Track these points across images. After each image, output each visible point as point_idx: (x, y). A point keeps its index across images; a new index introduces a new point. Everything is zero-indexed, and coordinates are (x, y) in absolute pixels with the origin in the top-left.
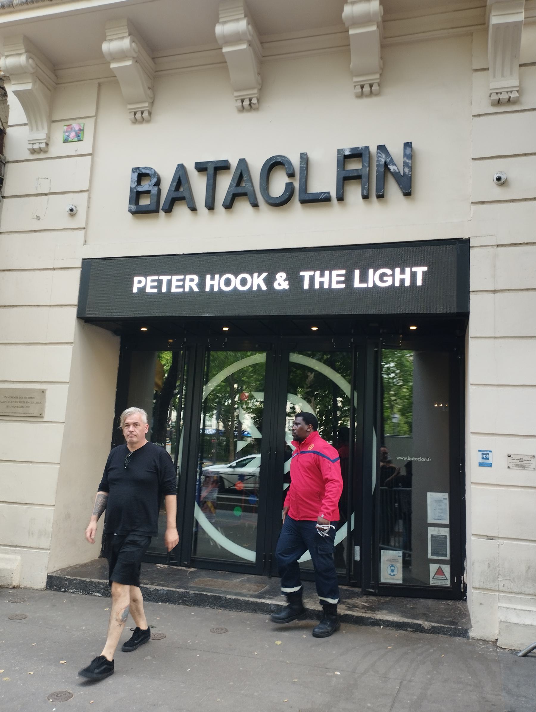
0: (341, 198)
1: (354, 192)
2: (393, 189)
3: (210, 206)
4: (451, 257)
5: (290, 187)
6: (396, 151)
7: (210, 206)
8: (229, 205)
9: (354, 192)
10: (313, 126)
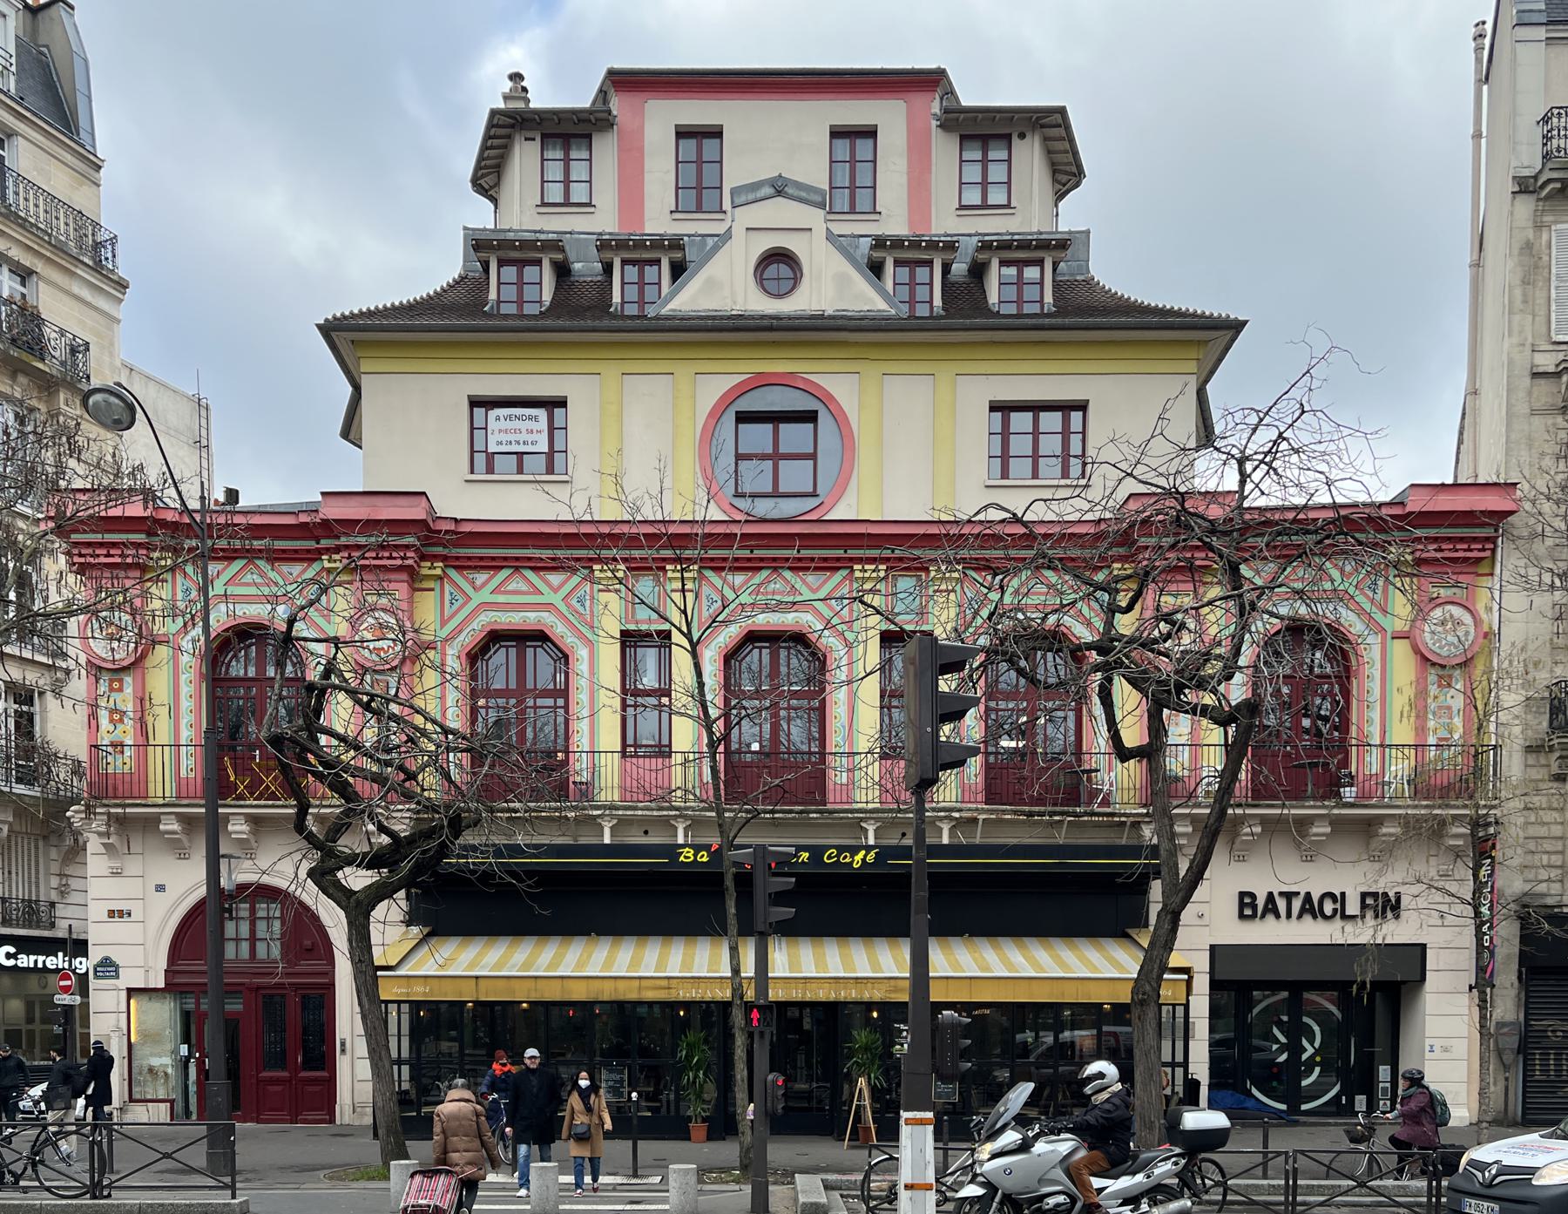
0: (1363, 917)
1: (1369, 914)
2: (1389, 914)
3: (1289, 916)
4: (1418, 952)
5: (1335, 911)
6: (1391, 894)
7: (1289, 916)
8: (1300, 916)
9: (1369, 914)
10: (1348, 878)
